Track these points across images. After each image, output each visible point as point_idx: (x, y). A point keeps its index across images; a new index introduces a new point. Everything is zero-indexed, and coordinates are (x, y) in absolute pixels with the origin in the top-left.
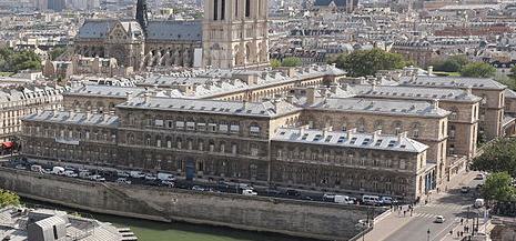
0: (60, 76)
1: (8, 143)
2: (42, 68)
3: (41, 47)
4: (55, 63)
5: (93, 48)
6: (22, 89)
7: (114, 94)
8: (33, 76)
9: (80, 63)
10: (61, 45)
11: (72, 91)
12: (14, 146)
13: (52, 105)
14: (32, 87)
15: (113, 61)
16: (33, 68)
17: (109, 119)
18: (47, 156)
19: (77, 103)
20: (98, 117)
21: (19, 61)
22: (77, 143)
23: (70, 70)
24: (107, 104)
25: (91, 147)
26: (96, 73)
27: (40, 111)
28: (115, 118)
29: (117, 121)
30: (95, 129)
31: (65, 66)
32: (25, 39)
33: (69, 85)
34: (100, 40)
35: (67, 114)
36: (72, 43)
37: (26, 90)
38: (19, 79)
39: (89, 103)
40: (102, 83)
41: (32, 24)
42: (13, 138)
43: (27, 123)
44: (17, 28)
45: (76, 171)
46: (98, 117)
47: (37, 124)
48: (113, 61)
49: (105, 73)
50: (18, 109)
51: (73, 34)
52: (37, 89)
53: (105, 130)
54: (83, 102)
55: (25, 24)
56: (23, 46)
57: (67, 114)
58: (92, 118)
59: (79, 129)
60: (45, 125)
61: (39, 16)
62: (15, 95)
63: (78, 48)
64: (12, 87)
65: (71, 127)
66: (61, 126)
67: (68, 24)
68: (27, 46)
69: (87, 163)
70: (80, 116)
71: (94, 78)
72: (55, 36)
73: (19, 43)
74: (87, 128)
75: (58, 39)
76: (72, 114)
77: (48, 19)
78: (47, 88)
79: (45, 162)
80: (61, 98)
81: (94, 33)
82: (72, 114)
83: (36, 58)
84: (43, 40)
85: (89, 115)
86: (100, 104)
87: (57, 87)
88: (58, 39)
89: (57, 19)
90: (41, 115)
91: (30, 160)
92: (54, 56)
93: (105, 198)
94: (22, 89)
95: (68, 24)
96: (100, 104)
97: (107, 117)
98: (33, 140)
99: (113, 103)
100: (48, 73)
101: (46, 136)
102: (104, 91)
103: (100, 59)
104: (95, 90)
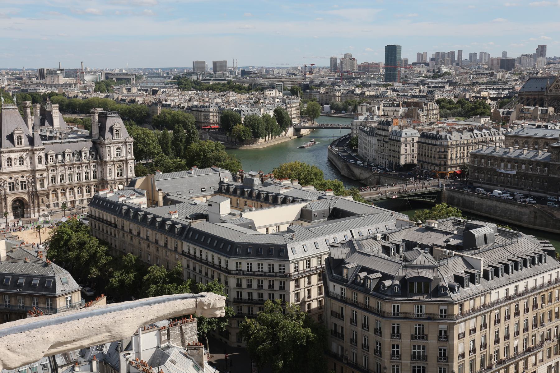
0: (505, 121)
1: (458, 170)
2: (490, 115)
3: (491, 99)
4: (501, 111)
5: (535, 99)
6: (471, 130)
7: (548, 135)
8: (483, 121)
9: (522, 111)
10: (509, 97)
11: (513, 133)
12: (463, 174)
13: (495, 141)
14: (480, 129)
15: (551, 110)
16: (483, 115)
17: (542, 155)
18: (489, 182)
19: (517, 142)
20: (532, 153)
21: (472, 109)
22: (514, 172)
23: (513, 116)
24: (541, 143)
25: (526, 176)
26: (535, 119)
27: (485, 148)
28: (547, 154)
29: (549, 156)
30: (529, 162)
31: (509, 113)
32: (479, 92)
33: (511, 127)
34: (541, 93)
35: (507, 150)
36: (517, 95)
37: (476, 131)
38: (471, 122)
39: (526, 142)
40: (539, 127)
41: (486, 80)
42: (463, 167)
43: (474, 156)
44: (474, 84)
45: (512, 195)
46: (532, 153)
47: (482, 157)
48: (551, 110)
49: (543, 119)
50: (468, 145)
51: (518, 88)
52: (484, 131)
53: (538, 163)
54: (521, 141)
55: (481, 81)
56: (476, 98)
57: (507, 150)
58: (527, 154)
59: (516, 162)
60: (488, 158)
61: (492, 75)
62: (466, 135)
63: (522, 99)
64: (464, 129)
65: (510, 160)
66: (501, 159)
67: (515, 80)
68: (480, 97)
69: (522, 189)
70: (518, 152)
71: (533, 123)
72: (504, 89)
73: (473, 95)
74: (524, 162)
75: (506, 92)
76: (512, 150)
77: (499, 76)
78: (493, 130)
79: (487, 186)
80: (503, 137)
81: (535, 87)
82: (512, 150)
83: (488, 107)
84: (493, 93)
85: (526, 152)
86: (536, 143)
87: (501, 129)
88: (506, 92)
89: (506, 76)
90: (485, 150)
91: (475, 184)
92: (501, 106)
93: (535, 217)
94: (471, 130)
95: (515, 80)
96: (536, 143)
97: (540, 153)
98: (478, 169)
99: (546, 142)
100: (495, 118)
101: (489, 166)
102: (540, 133)
103: (540, 108)
104: (532, 132)
